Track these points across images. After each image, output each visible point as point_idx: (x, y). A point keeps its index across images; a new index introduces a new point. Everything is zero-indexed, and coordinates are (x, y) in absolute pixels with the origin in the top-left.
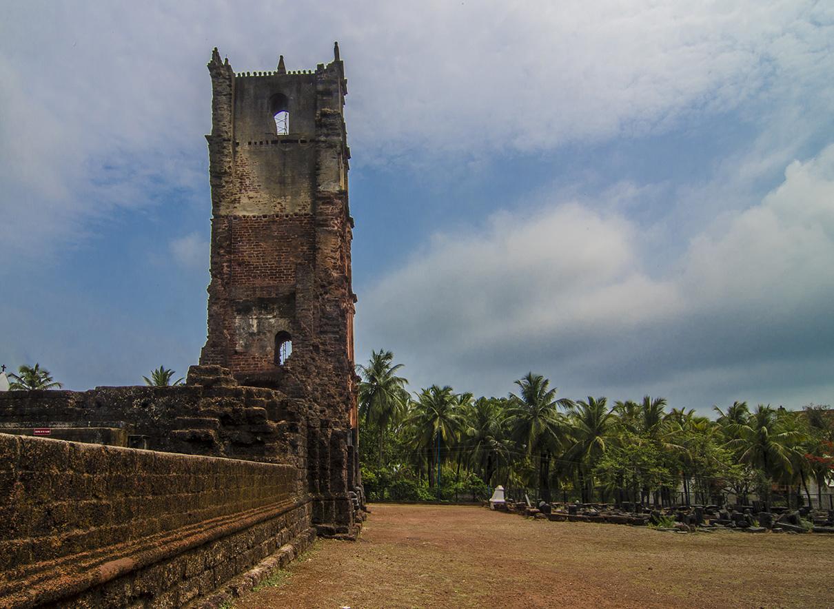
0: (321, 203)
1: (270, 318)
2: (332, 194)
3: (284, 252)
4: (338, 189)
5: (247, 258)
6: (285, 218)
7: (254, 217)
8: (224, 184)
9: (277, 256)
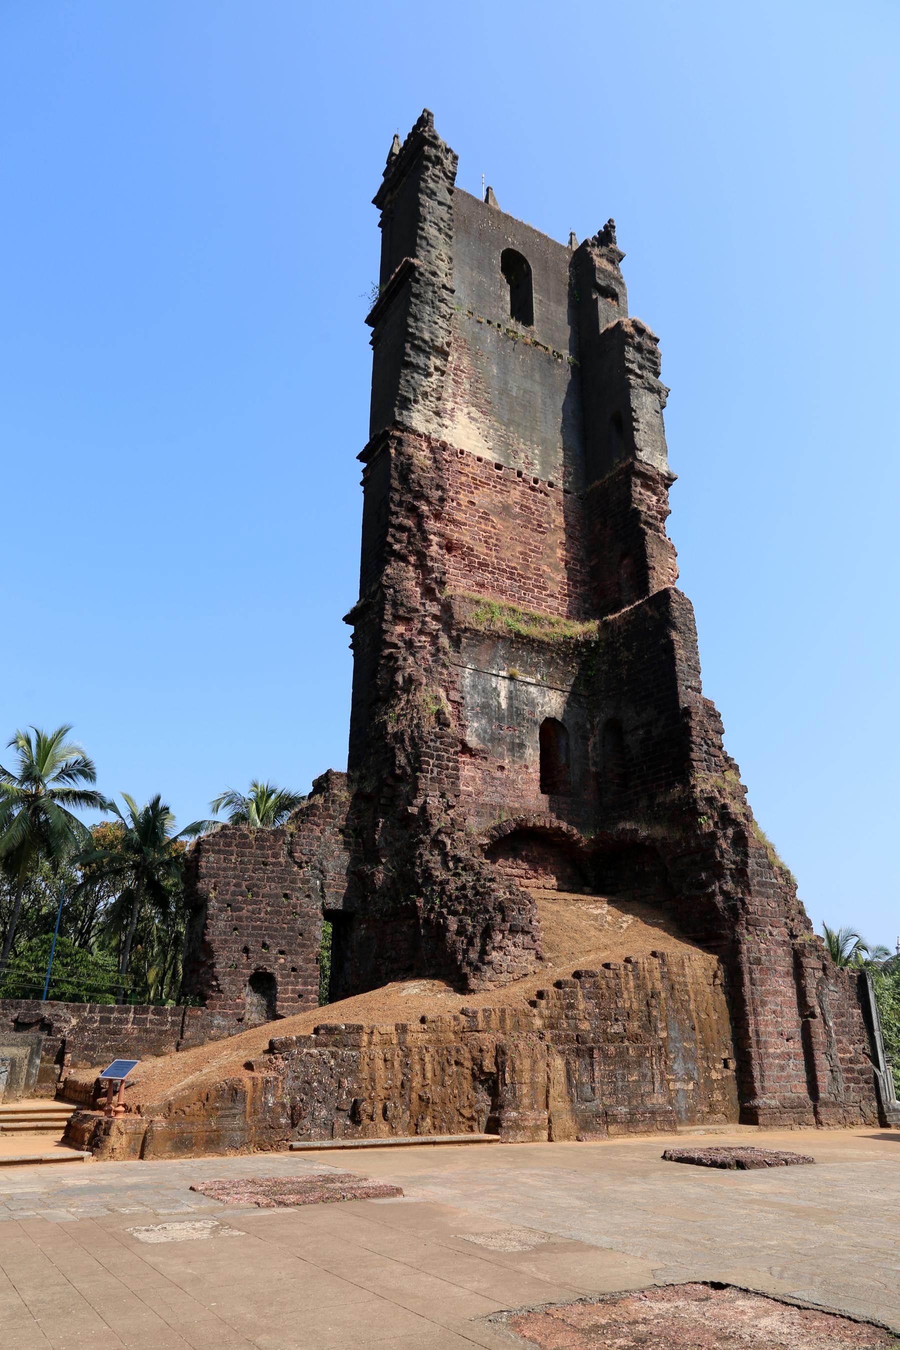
0: (638, 482)
1: (529, 683)
2: (658, 474)
3: (533, 551)
5: (468, 539)
6: (532, 484)
7: (480, 460)
8: (432, 370)
9: (521, 553)
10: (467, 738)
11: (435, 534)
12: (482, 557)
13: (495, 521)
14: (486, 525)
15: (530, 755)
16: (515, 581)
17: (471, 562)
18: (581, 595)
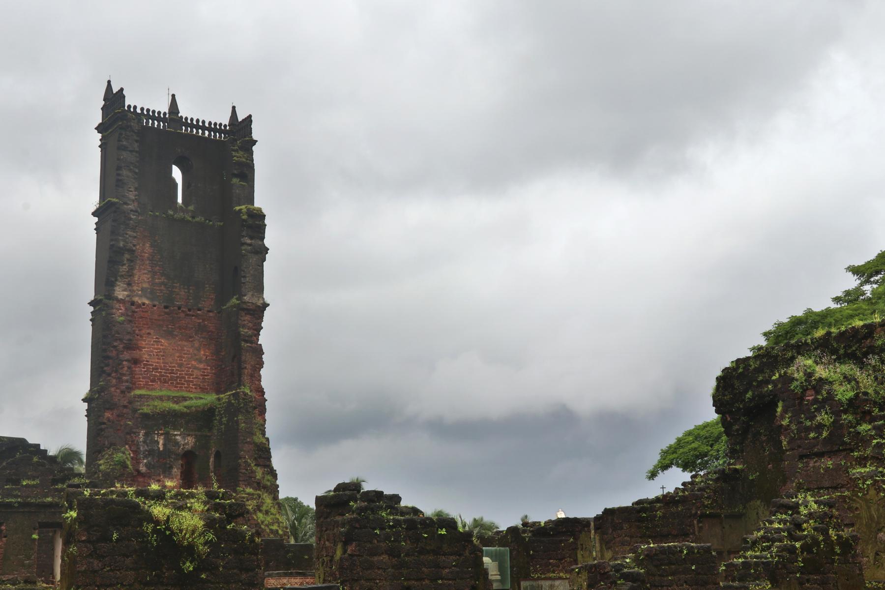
0: (243, 313)
1: (176, 435)
3: (185, 354)
4: (262, 302)
9: (178, 357)
10: (141, 469)
11: (126, 361)
12: (154, 364)
13: (163, 341)
14: (158, 345)
15: (175, 472)
16: (174, 373)
17: (148, 369)
18: (214, 374)
